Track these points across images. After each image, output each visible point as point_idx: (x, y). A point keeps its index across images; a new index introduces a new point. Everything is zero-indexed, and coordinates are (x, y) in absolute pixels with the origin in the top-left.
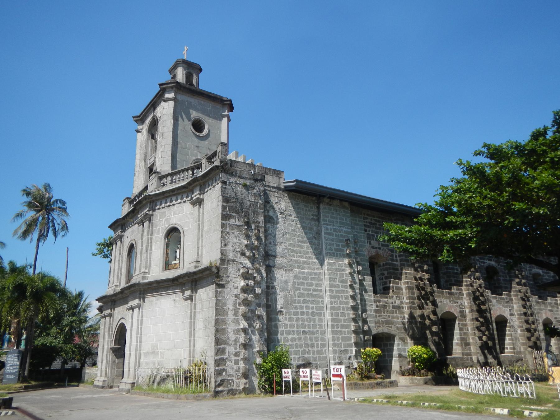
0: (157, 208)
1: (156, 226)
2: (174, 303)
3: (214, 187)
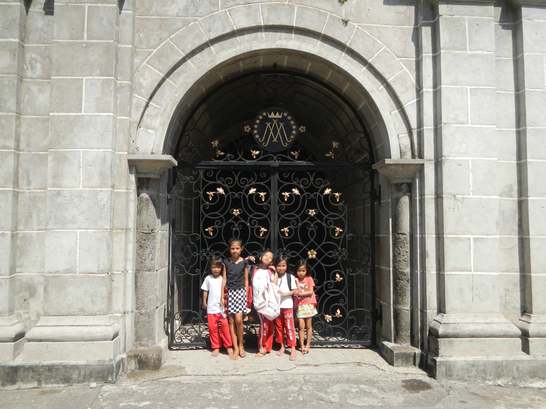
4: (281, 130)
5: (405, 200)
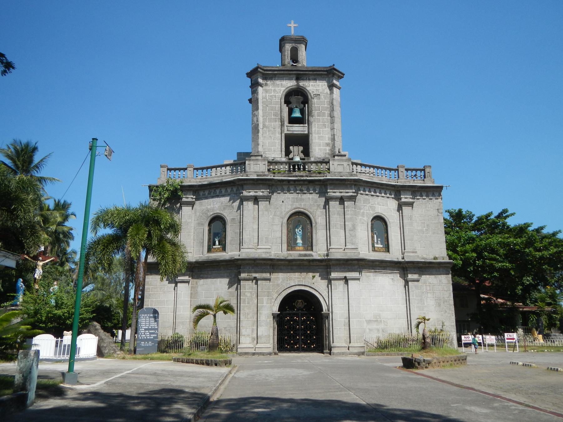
0: (359, 192)
1: (360, 209)
2: (393, 281)
3: (431, 199)
5: (327, 320)
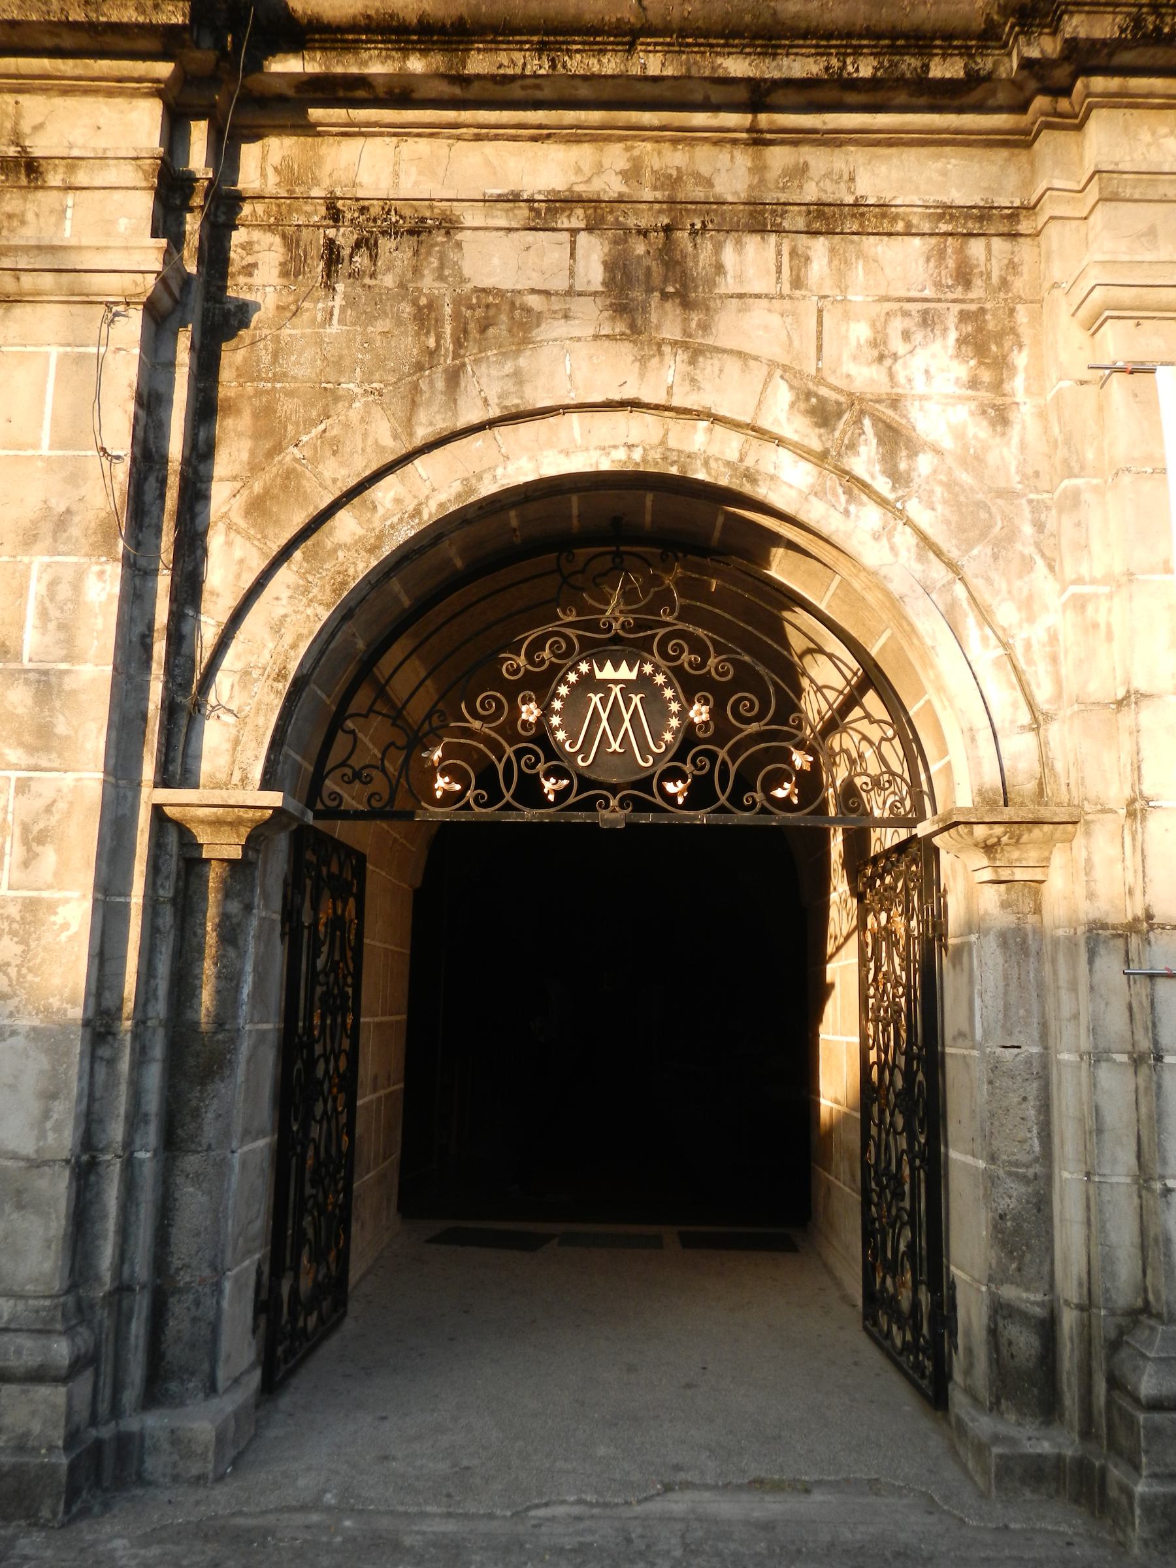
4: (635, 717)
